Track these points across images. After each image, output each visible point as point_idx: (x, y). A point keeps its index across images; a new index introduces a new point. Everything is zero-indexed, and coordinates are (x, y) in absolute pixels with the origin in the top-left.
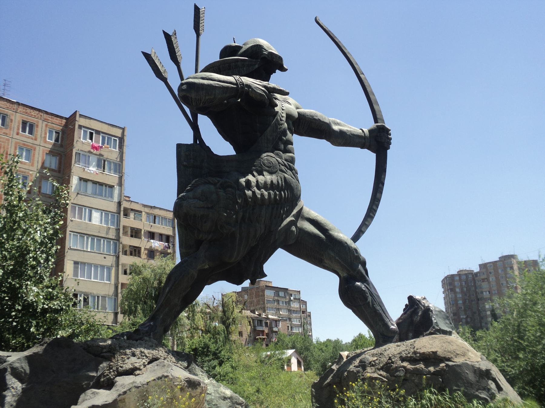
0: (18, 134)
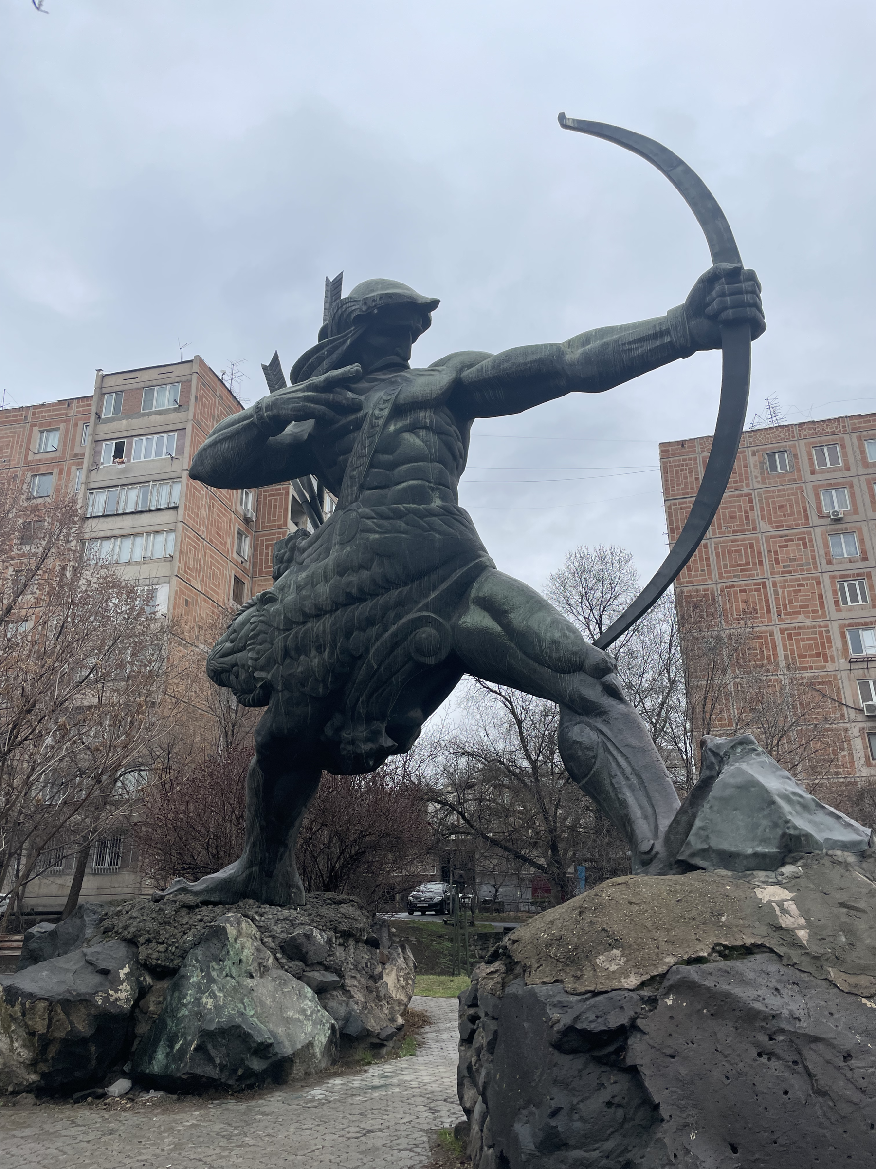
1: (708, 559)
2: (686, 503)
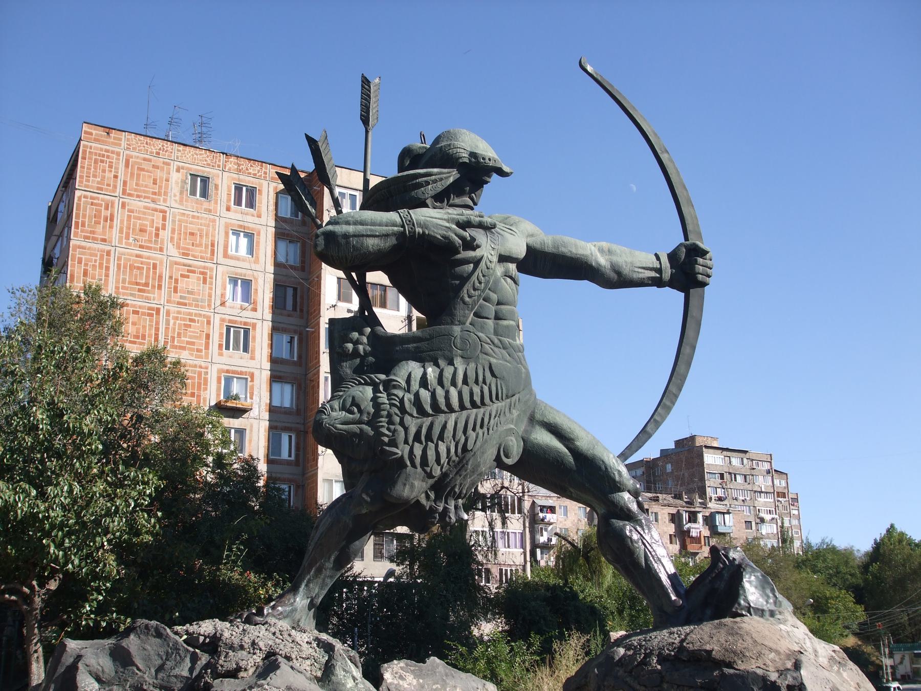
0: (228, 209)
1: (108, 268)
2: (98, 198)
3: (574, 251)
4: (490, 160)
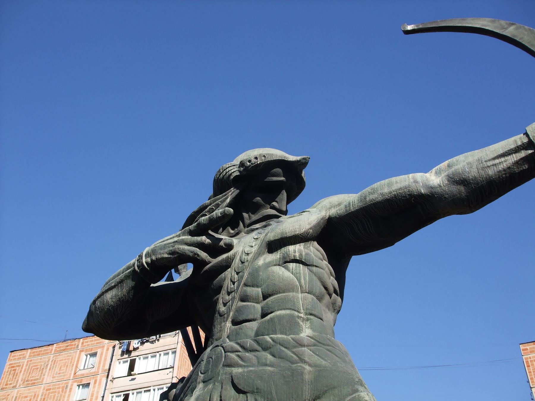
3: (386, 190)
4: (256, 158)
